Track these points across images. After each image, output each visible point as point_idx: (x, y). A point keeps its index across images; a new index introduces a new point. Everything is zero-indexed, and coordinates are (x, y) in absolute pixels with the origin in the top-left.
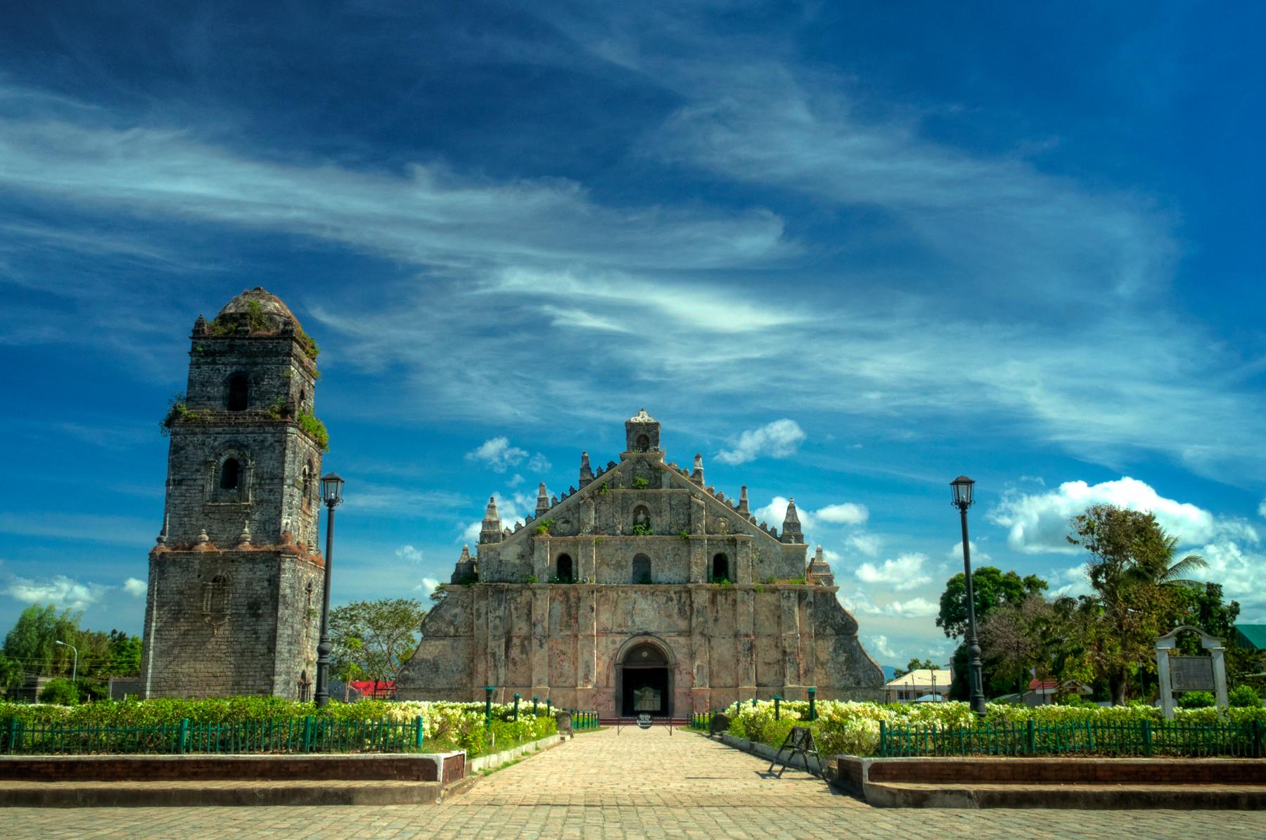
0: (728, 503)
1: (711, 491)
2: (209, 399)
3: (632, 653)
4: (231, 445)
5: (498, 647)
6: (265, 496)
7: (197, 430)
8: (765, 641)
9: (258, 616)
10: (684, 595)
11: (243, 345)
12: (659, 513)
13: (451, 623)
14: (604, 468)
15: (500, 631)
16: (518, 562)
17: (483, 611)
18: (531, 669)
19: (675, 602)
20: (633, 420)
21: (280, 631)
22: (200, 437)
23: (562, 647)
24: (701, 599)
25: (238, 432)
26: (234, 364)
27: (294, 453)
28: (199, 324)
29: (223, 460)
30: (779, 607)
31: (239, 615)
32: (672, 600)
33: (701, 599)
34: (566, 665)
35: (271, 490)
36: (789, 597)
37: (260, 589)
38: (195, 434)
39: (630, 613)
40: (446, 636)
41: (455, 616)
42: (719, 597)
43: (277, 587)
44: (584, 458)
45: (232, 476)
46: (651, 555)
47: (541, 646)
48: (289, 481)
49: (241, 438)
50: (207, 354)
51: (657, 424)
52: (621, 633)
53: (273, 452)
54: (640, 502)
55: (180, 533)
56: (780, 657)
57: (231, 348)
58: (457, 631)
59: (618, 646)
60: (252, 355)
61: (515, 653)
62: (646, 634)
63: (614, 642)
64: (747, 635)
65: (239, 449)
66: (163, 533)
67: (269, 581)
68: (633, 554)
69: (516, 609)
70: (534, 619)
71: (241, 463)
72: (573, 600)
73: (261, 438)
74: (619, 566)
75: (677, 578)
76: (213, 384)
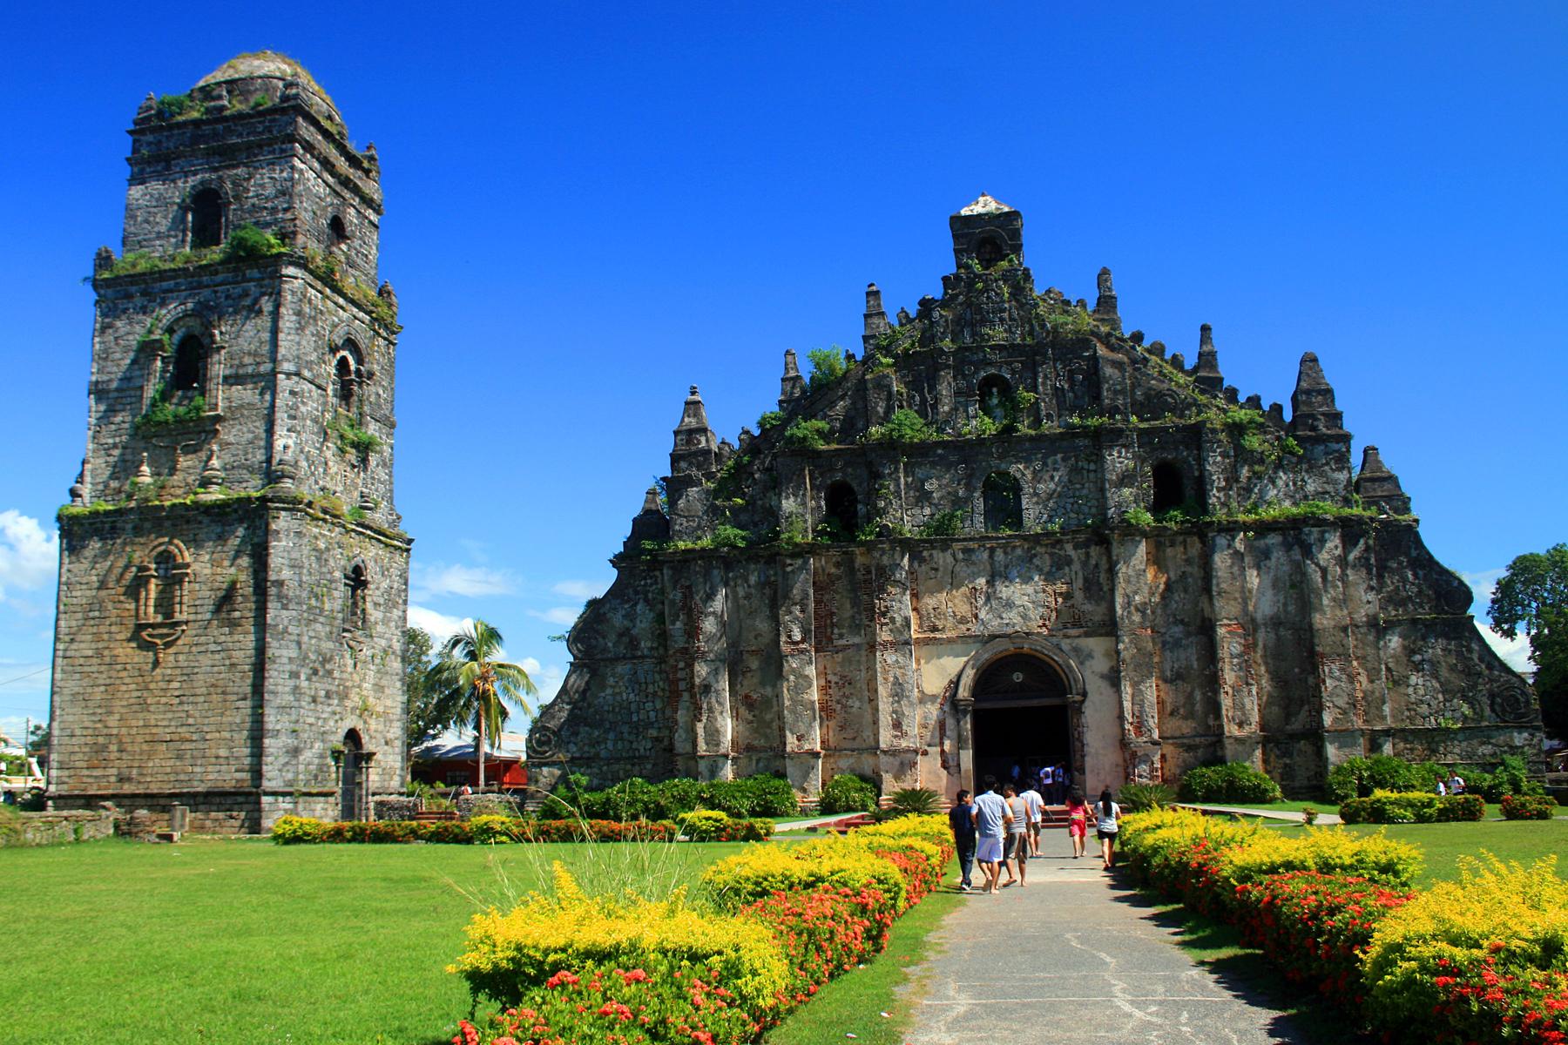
0: (1176, 362)
3: (990, 677)
7: (133, 289)
10: (1094, 551)
19: (1076, 566)
20: (965, 212)
21: (269, 653)
27: (299, 313)
32: (1069, 562)
44: (873, 295)
45: (189, 364)
48: (288, 366)
51: (1014, 215)
66: (80, 479)
69: (748, 597)
71: (206, 341)
73: (238, 290)
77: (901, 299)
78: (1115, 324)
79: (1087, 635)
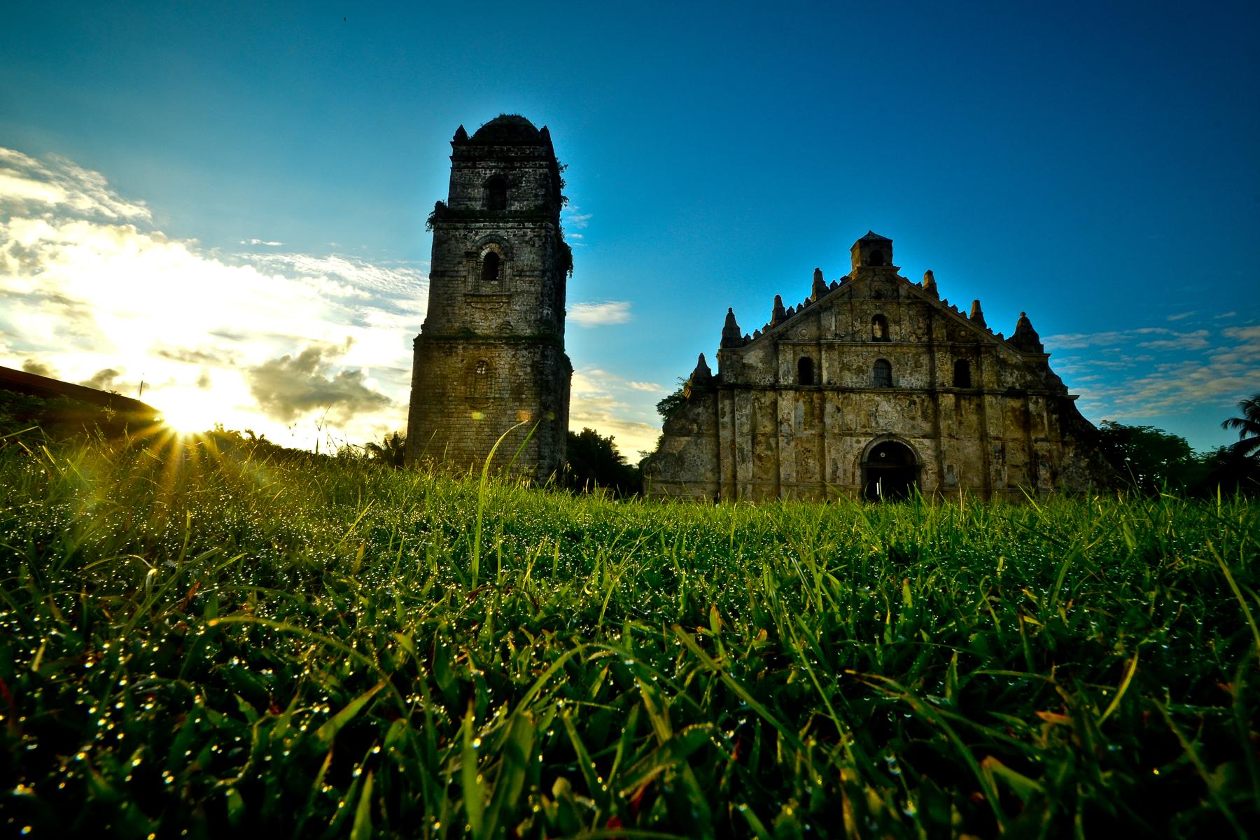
1: (946, 302)
2: (470, 199)
4: (491, 239)
5: (744, 442)
6: (526, 287)
7: (459, 225)
8: (1010, 444)
9: (521, 400)
11: (502, 150)
12: (898, 323)
13: (695, 421)
14: (839, 282)
15: (746, 429)
16: (760, 365)
17: (727, 409)
18: (778, 465)
19: (918, 406)
22: (462, 232)
23: (807, 446)
24: (948, 401)
25: (499, 228)
26: (491, 168)
28: (461, 132)
29: (484, 253)
30: (1026, 412)
31: (502, 399)
33: (948, 401)
34: (811, 462)
35: (531, 282)
36: (1037, 403)
37: (524, 374)
38: (457, 229)
39: (874, 415)
40: (689, 433)
41: (698, 414)
42: (963, 402)
43: (541, 373)
46: (892, 360)
47: (788, 443)
49: (501, 232)
50: (467, 159)
52: (866, 434)
53: (533, 246)
54: (878, 312)
55: (444, 320)
56: (1027, 460)
57: (489, 156)
58: (699, 428)
59: (863, 445)
60: (512, 160)
61: (760, 449)
62: (891, 435)
63: (858, 442)
64: (997, 438)
65: (499, 243)
67: (532, 366)
68: (874, 360)
70: (780, 417)
72: (816, 401)
74: (860, 371)
75: (919, 384)
76: (474, 186)
77: (832, 277)
78: (937, 296)
79: (924, 437)
